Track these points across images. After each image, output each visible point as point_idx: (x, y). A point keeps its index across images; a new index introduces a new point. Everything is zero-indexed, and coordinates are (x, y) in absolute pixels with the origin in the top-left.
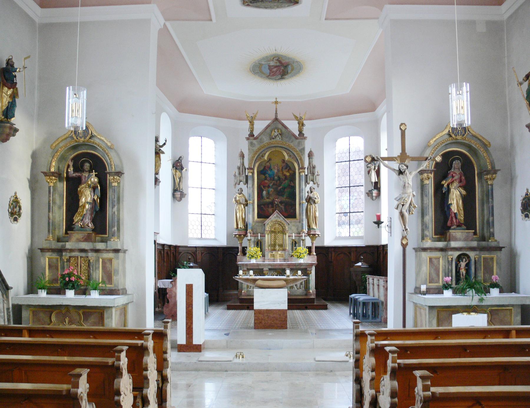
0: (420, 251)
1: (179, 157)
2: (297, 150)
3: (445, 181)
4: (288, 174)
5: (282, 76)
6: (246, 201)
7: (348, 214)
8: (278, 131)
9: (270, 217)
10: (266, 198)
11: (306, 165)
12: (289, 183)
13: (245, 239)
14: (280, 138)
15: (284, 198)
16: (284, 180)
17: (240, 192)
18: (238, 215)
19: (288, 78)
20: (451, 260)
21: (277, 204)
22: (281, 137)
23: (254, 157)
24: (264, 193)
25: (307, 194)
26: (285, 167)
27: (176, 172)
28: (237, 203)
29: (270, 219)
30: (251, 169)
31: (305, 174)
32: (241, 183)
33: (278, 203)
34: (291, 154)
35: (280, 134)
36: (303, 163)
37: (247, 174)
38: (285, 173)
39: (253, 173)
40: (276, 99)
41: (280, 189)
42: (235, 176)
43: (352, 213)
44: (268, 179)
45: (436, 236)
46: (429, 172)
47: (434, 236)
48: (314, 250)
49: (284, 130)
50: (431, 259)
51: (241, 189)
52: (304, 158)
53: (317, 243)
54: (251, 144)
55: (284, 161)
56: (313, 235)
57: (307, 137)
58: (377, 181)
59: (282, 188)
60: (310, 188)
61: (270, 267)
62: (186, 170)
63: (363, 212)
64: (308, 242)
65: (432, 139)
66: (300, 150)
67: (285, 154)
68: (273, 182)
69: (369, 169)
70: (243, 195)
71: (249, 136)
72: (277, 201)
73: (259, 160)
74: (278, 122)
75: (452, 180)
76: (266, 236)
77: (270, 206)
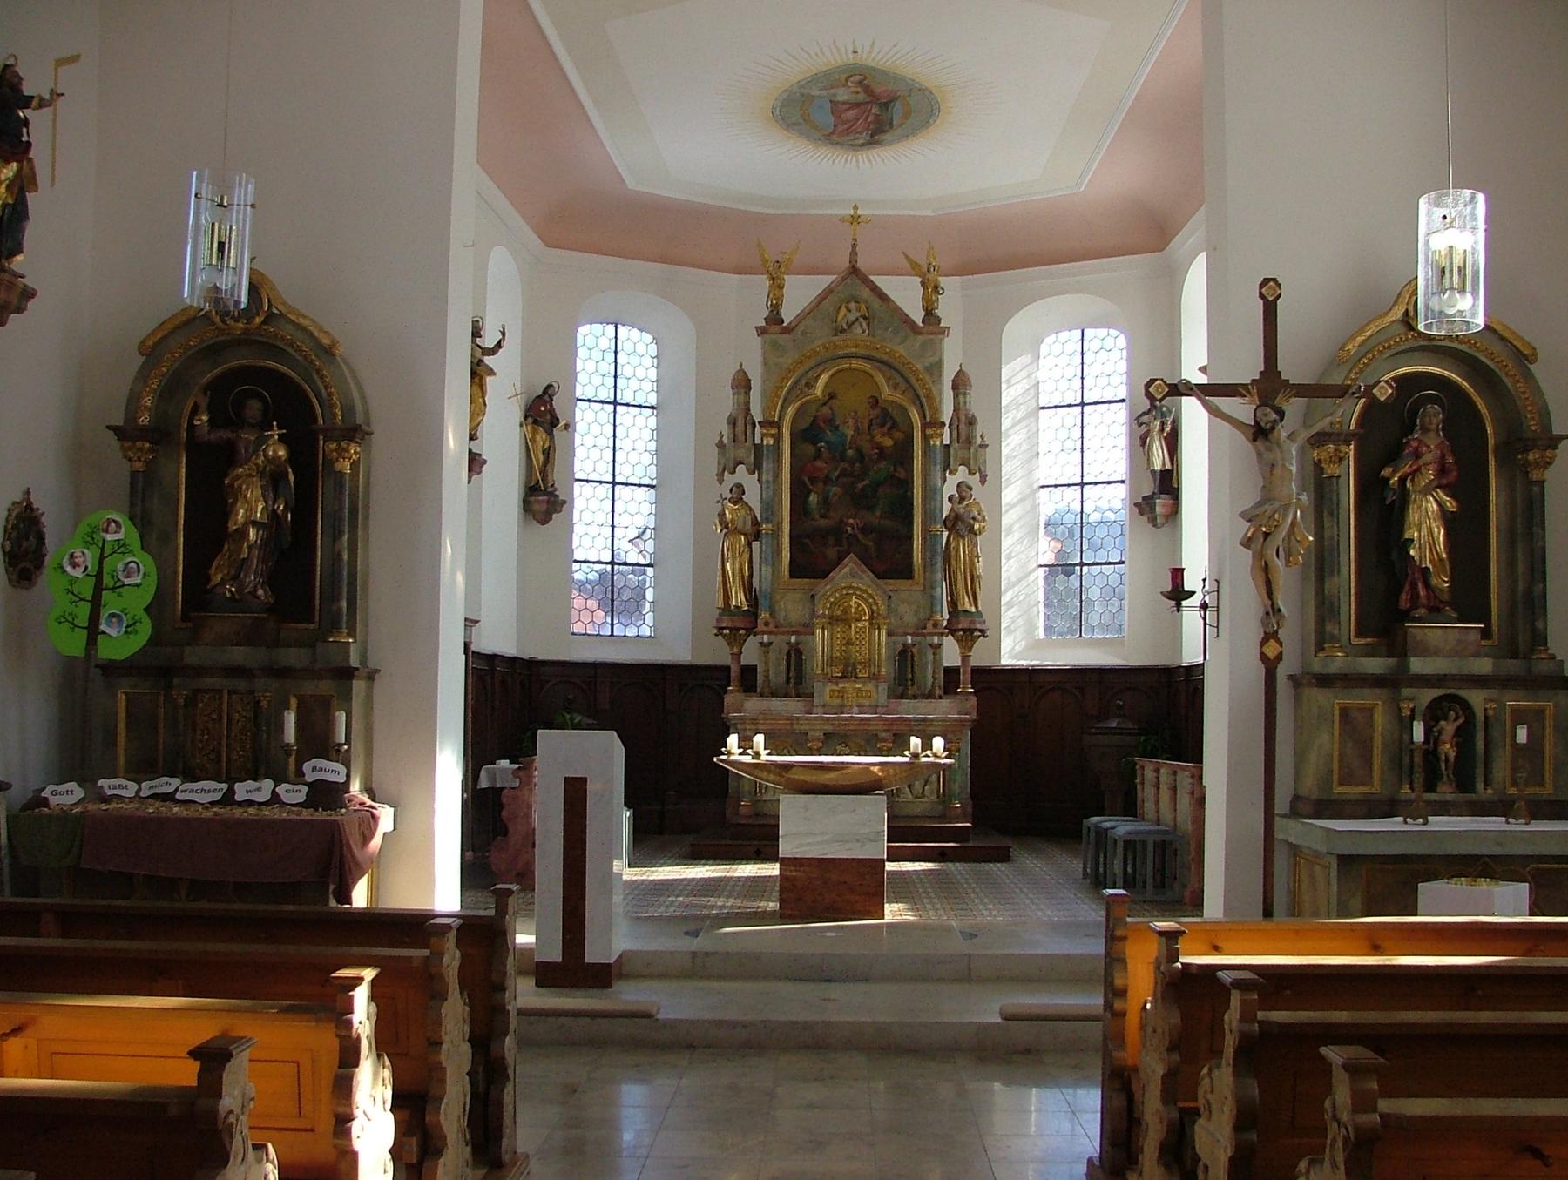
0: (1310, 685)
1: (545, 385)
3: (1391, 469)
4: (888, 442)
5: (872, 136)
6: (755, 523)
7: (1078, 568)
8: (859, 310)
10: (818, 516)
11: (947, 415)
12: (892, 469)
14: (864, 332)
15: (875, 518)
18: (728, 565)
19: (891, 143)
20: (1409, 713)
22: (868, 325)
23: (782, 388)
24: (813, 498)
25: (947, 507)
26: (878, 421)
27: (534, 432)
28: (725, 531)
31: (942, 441)
32: (741, 468)
34: (899, 380)
35: (865, 318)
36: (936, 410)
37: (758, 441)
38: (878, 438)
39: (778, 438)
40: (855, 207)
41: (863, 489)
42: (721, 445)
43: (1088, 564)
45: (1363, 641)
46: (1342, 437)
47: (1355, 641)
48: (965, 677)
49: (876, 303)
50: (1344, 712)
51: (739, 486)
52: (941, 393)
53: (979, 658)
54: (771, 350)
55: (875, 402)
56: (963, 630)
58: (1168, 466)
61: (829, 728)
62: (567, 427)
63: (1123, 563)
64: (951, 653)
65: (1353, 338)
67: (880, 379)
69: (1143, 429)
70: (747, 504)
71: (767, 323)
74: (858, 281)
75: (1415, 467)
76: (819, 631)
77: (831, 540)
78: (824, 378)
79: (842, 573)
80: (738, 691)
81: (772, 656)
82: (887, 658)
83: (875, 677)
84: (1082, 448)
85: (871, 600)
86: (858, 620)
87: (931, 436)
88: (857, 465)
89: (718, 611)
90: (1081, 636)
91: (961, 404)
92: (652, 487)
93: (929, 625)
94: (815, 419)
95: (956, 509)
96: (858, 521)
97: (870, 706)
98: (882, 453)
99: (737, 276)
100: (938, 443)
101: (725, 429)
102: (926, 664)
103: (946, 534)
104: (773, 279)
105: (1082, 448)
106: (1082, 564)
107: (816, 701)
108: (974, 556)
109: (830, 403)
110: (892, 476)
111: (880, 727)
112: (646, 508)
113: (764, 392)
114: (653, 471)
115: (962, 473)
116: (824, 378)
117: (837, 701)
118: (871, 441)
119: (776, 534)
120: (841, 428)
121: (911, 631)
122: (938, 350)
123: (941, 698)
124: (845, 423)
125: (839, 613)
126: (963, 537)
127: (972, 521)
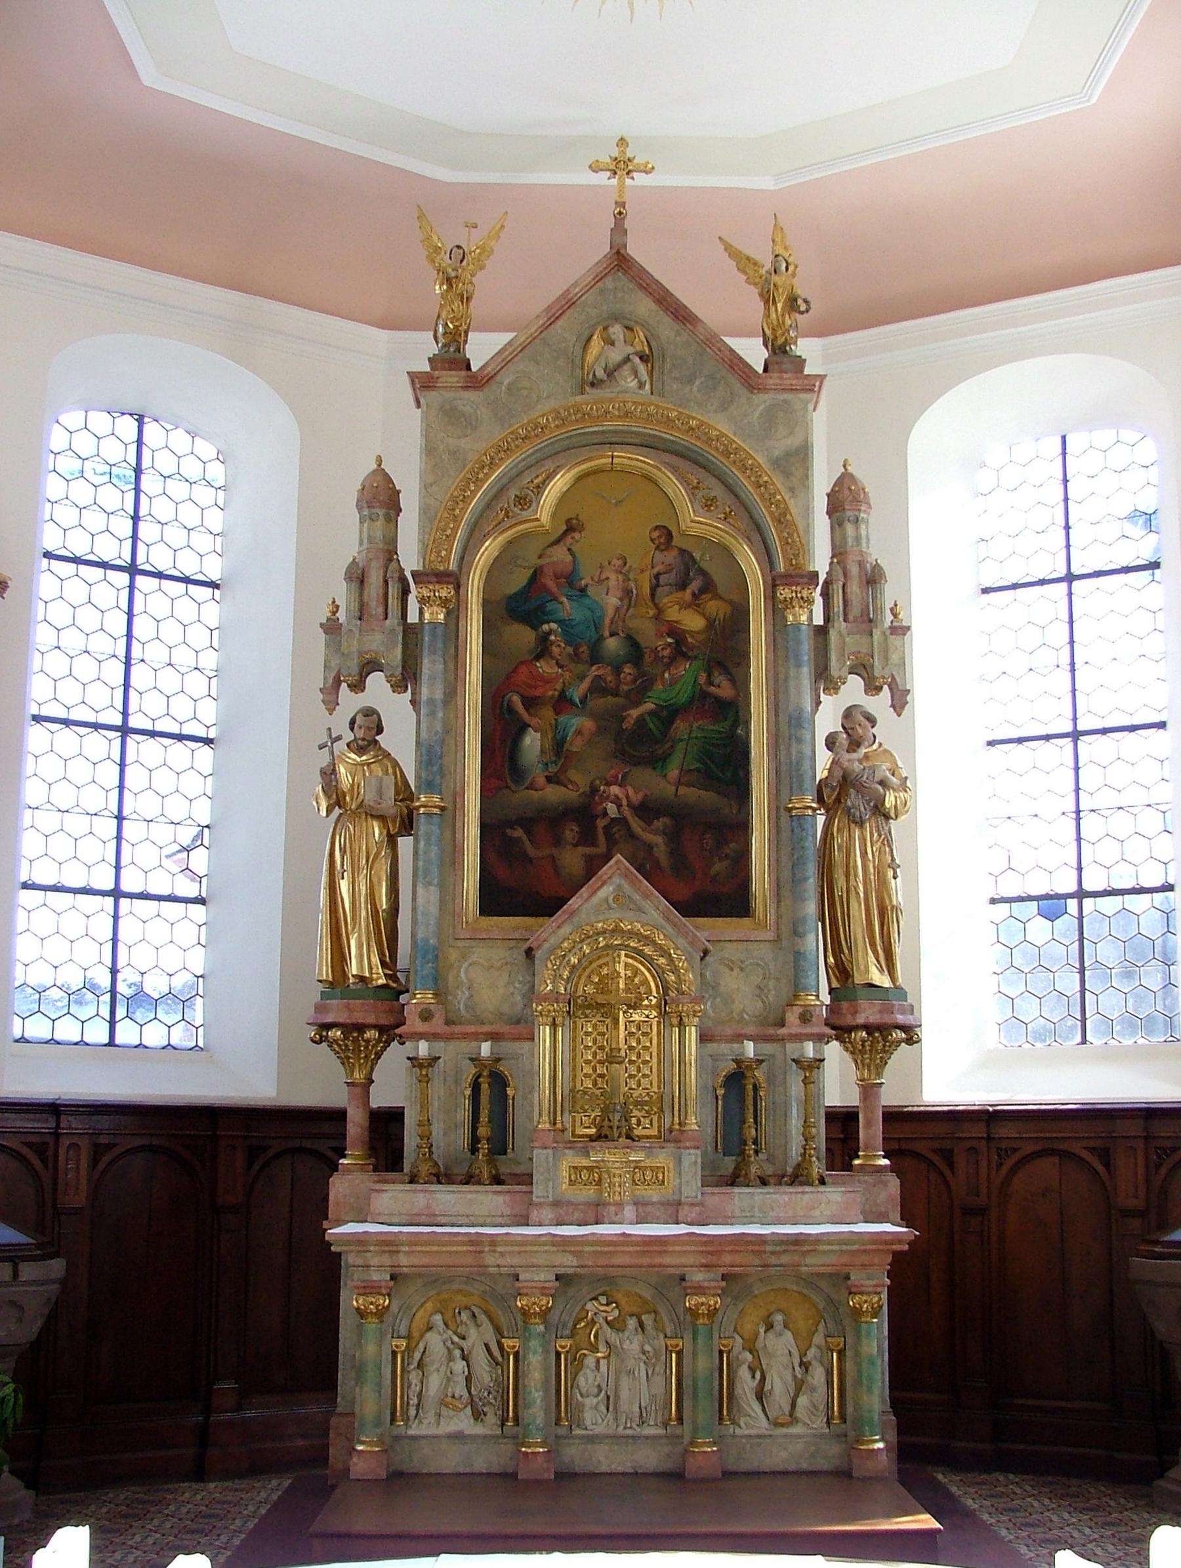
2: (761, 459)
4: (693, 622)
6: (405, 794)
9: (574, 902)
10: (541, 780)
11: (821, 562)
12: (703, 678)
13: (395, 1055)
14: (641, 385)
16: (672, 660)
17: (360, 734)
18: (344, 886)
21: (622, 821)
22: (651, 374)
24: (532, 743)
25: (823, 759)
29: (572, 914)
30: (442, 577)
31: (810, 619)
32: (376, 681)
33: (627, 811)
34: (718, 491)
35: (643, 358)
36: (798, 547)
37: (413, 618)
39: (455, 611)
41: (641, 721)
42: (331, 627)
44: (555, 650)
48: (871, 1132)
49: (666, 329)
52: (807, 511)
53: (892, 1095)
55: (665, 537)
57: (822, 378)
59: (651, 713)
60: (848, 714)
61: (568, 1262)
66: (776, 463)
67: (675, 488)
68: (594, 671)
70: (387, 755)
72: (617, 801)
73: (498, 528)
77: (571, 832)
78: (560, 483)
79: (595, 900)
80: (362, 1168)
81: (437, 1089)
82: (702, 1088)
83: (673, 1137)
84: (1072, 664)
85: (662, 961)
86: (634, 1006)
87: (788, 603)
88: (628, 669)
89: (321, 987)
90: (1084, 1041)
91: (850, 541)
92: (208, 741)
93: (792, 1017)
94: (536, 576)
95: (846, 764)
96: (631, 791)
97: (663, 1204)
98: (681, 647)
99: (382, 336)
100: (804, 618)
101: (341, 592)
102: (786, 1106)
103: (821, 820)
104: (449, 281)
105: (1072, 664)
106: (1081, 894)
107: (538, 1190)
108: (886, 867)
109: (569, 540)
110: (705, 695)
111: (690, 1260)
112: (193, 784)
113: (425, 511)
114: (208, 711)
115: (853, 690)
116: (560, 483)
117: (589, 1193)
118: (658, 616)
119: (450, 814)
120: (590, 591)
121: (751, 1030)
122: (799, 422)
123: (822, 1182)
124: (600, 582)
125: (590, 989)
126: (861, 824)
127: (880, 787)
